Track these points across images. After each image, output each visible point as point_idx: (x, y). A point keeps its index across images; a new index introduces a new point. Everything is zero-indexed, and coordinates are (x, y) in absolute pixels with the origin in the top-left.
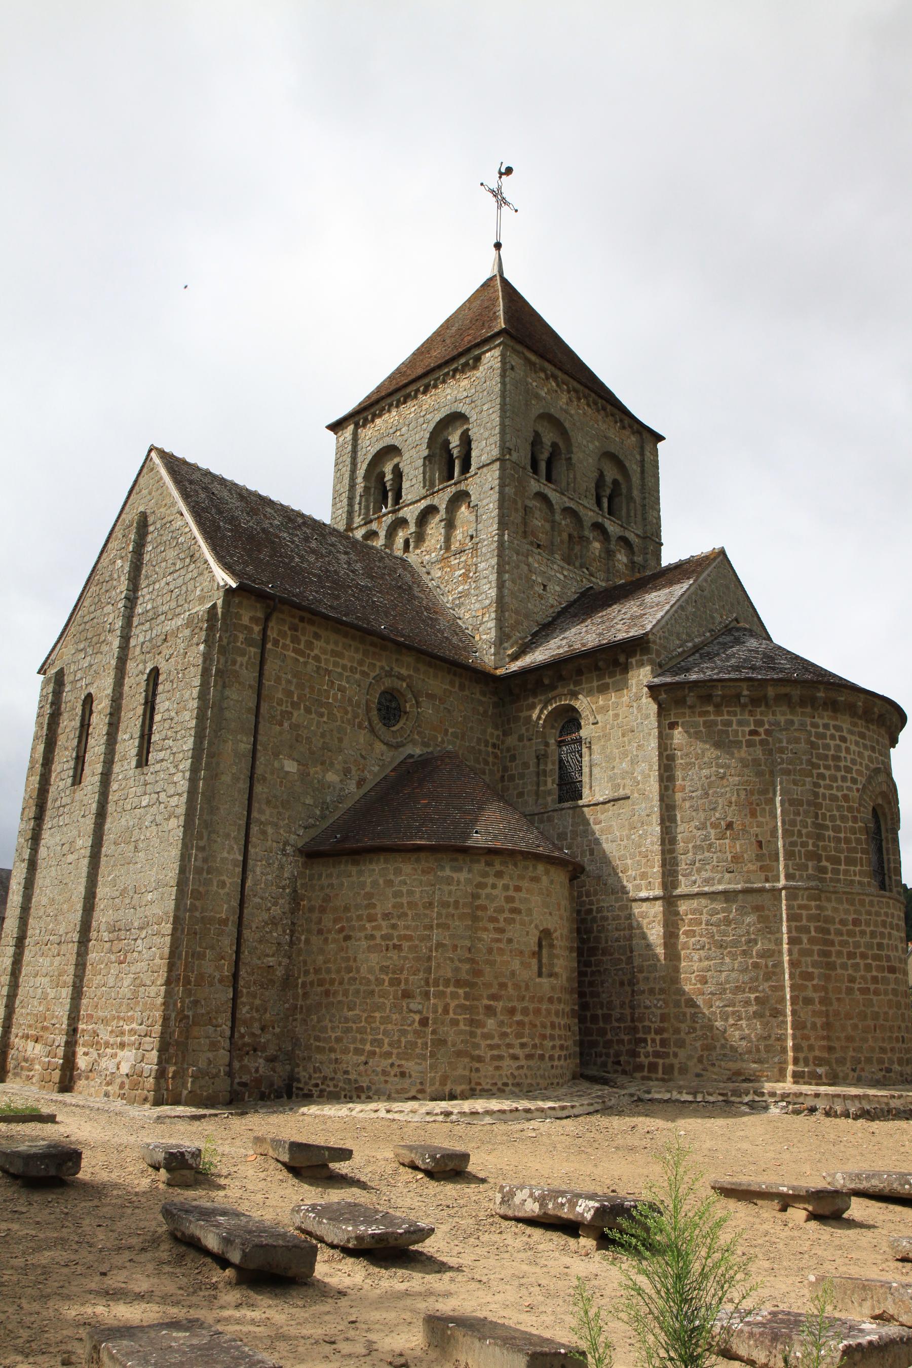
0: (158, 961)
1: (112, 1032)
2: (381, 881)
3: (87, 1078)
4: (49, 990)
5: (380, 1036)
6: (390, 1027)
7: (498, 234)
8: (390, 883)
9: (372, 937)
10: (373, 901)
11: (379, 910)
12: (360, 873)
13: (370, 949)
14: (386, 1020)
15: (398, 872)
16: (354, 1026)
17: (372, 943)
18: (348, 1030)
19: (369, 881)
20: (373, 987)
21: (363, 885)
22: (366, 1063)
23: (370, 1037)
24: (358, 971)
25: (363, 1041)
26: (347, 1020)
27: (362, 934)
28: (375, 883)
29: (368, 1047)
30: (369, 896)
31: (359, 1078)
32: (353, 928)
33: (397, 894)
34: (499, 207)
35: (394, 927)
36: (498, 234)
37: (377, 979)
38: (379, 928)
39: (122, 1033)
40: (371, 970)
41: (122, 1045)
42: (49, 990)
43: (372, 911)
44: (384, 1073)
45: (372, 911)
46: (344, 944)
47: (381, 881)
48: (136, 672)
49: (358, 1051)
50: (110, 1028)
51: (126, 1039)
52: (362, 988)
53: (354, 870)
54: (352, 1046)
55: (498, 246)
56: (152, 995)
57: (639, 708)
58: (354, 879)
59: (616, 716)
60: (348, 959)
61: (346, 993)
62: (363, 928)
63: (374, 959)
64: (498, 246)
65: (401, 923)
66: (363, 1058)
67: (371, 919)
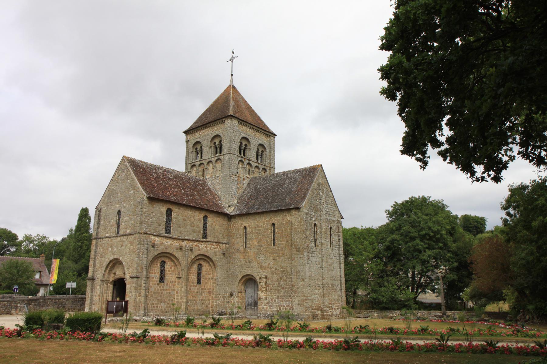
7: (232, 71)
34: (230, 60)
36: (232, 71)
55: (232, 75)
64: (232, 75)
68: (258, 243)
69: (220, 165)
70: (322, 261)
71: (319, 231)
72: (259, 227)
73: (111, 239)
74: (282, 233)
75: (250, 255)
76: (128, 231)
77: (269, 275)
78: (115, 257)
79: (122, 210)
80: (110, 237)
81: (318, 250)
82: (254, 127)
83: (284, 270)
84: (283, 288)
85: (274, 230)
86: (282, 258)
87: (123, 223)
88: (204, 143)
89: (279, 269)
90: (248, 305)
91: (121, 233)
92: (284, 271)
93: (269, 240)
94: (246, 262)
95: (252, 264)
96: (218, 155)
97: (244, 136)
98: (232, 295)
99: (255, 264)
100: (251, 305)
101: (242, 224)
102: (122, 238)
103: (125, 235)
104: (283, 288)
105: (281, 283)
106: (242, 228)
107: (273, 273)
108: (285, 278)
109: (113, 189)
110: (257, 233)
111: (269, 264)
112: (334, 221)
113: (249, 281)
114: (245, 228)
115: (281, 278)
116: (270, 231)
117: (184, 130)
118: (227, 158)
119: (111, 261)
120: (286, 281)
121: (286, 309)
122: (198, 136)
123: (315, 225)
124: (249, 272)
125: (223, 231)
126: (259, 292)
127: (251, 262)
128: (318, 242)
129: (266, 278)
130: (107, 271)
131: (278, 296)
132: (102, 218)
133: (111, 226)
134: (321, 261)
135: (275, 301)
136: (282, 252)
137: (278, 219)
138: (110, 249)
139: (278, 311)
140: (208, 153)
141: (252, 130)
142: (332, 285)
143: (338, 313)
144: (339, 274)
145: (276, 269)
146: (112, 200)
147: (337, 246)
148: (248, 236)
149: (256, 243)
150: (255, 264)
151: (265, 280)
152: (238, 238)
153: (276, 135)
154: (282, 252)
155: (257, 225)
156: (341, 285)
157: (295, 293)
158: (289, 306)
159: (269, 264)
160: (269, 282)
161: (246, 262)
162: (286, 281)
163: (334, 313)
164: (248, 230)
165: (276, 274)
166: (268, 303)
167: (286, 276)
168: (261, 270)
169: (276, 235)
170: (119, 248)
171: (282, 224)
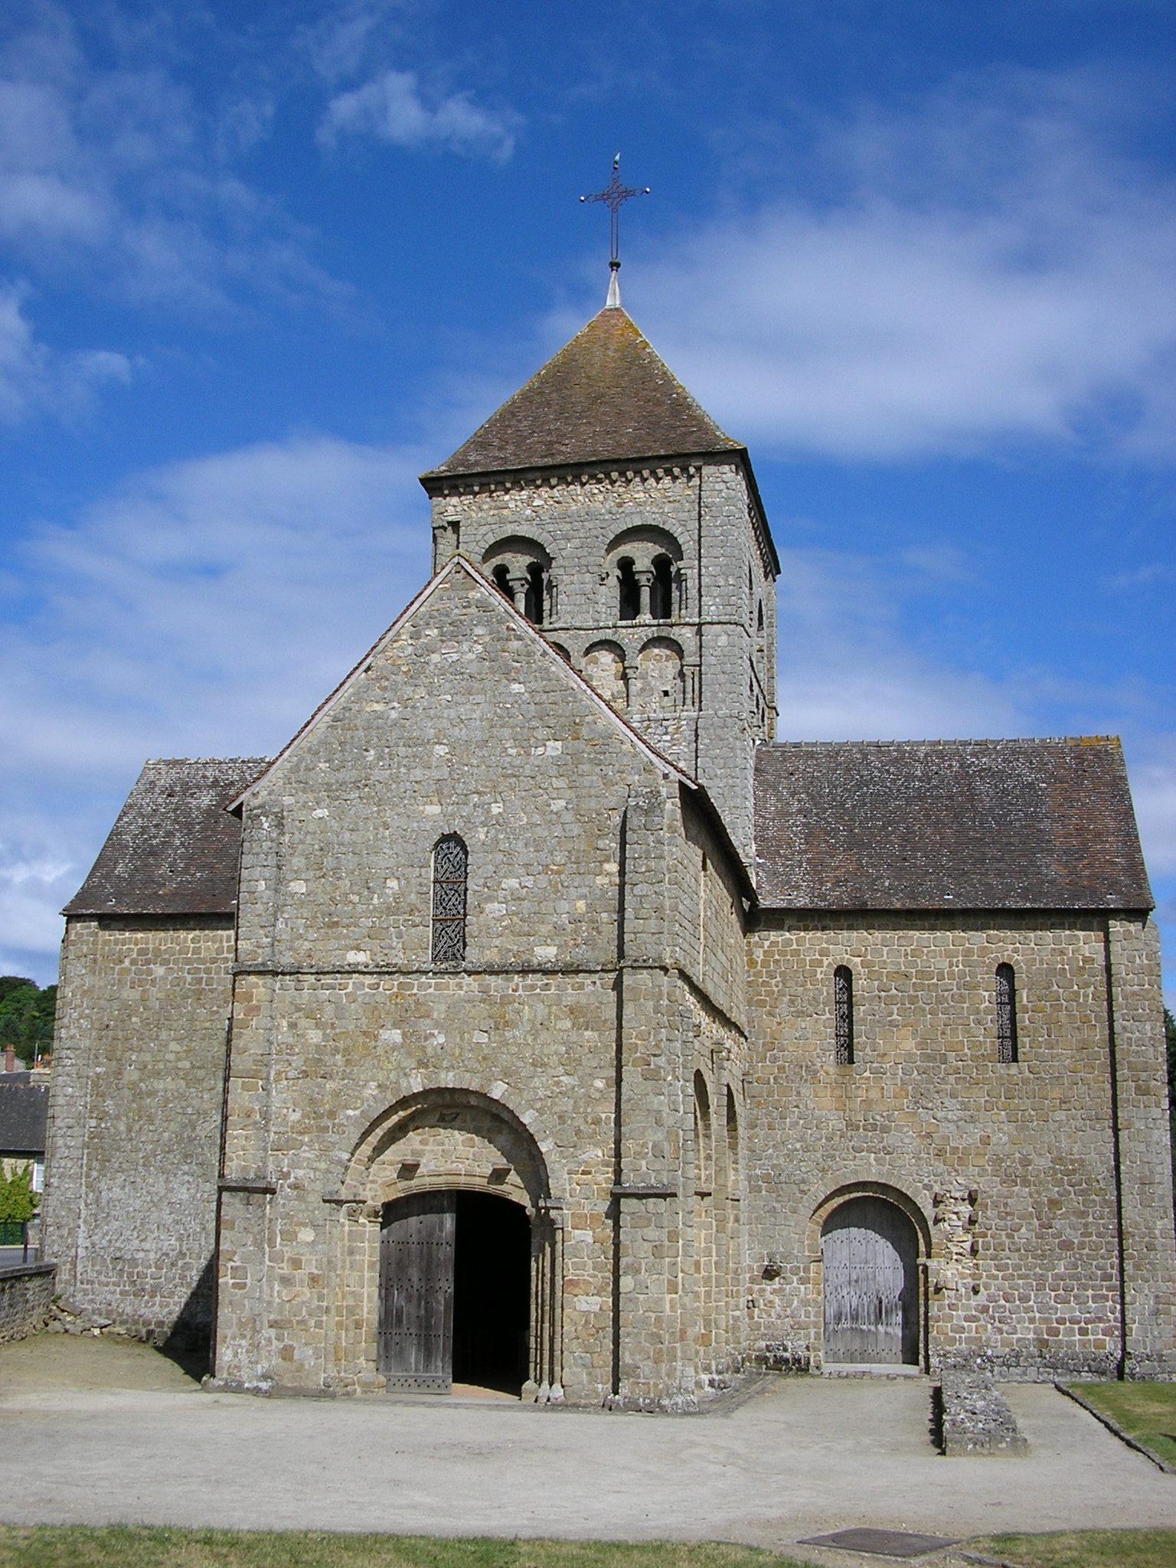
68: (921, 1045)
69: (671, 667)
72: (922, 974)
73: (393, 983)
74: (1057, 1008)
75: (874, 1094)
76: (547, 953)
77: (989, 1186)
78: (448, 1079)
79: (477, 837)
80: (385, 971)
83: (1067, 1169)
84: (1067, 1245)
85: (1012, 993)
86: (1061, 1115)
87: (494, 908)
88: (562, 550)
89: (1043, 1162)
90: (838, 1318)
91: (473, 955)
92: (1068, 1173)
93: (986, 1035)
94: (851, 1125)
95: (890, 1139)
96: (646, 617)
98: (769, 1274)
99: (906, 1138)
100: (855, 1318)
101: (824, 953)
102: (492, 981)
103: (524, 972)
104: (1067, 1245)
105: (1057, 1224)
106: (824, 972)
107: (1009, 1180)
108: (1075, 1201)
109: (380, 716)
110: (913, 1000)
111: (986, 1141)
113: (882, 1210)
114: (843, 973)
115: (1054, 1204)
116: (987, 997)
117: (422, 475)
118: (723, 640)
119: (403, 1103)
120: (1083, 1214)
121: (1083, 1332)
122: (521, 510)
124: (873, 1173)
126: (932, 1264)
127: (885, 1130)
129: (972, 1199)
130: (366, 1149)
131: (1041, 1277)
132: (298, 862)
133: (390, 911)
135: (1024, 1299)
136: (1057, 1093)
137: (1027, 948)
138: (395, 1035)
139: (1042, 1343)
140: (585, 598)
145: (1026, 1162)
146: (377, 775)
148: (859, 1012)
149: (910, 1045)
150: (906, 1138)
151: (965, 1209)
152: (800, 1014)
154: (1057, 1093)
155: (908, 964)
157: (1137, 1267)
158: (1100, 1320)
159: (986, 1141)
160: (989, 1217)
161: (851, 1125)
162: (1083, 1214)
164: (859, 984)
165: (1025, 1183)
166: (985, 1309)
167: (1083, 1192)
168: (941, 1168)
169: (1023, 1019)
170: (484, 1038)
171: (1052, 971)
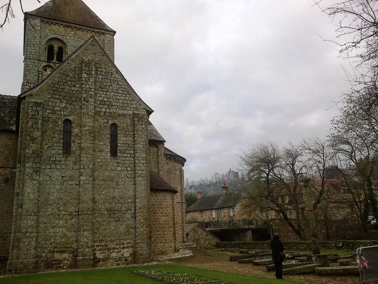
0: (142, 220)
1: (117, 244)
2: (163, 198)
3: (104, 261)
4: (67, 233)
5: (167, 238)
6: (168, 235)
8: (165, 199)
9: (162, 213)
10: (162, 203)
11: (163, 206)
12: (157, 196)
13: (162, 216)
14: (167, 234)
15: (166, 196)
16: (160, 236)
17: (162, 214)
18: (158, 237)
19: (160, 198)
20: (164, 225)
21: (158, 199)
22: (164, 245)
23: (164, 239)
24: (159, 221)
25: (162, 240)
26: (157, 235)
27: (160, 212)
28: (161, 199)
29: (164, 241)
30: (160, 202)
31: (162, 250)
32: (156, 210)
33: (167, 202)
35: (167, 210)
37: (164, 224)
38: (164, 210)
39: (124, 244)
40: (163, 221)
41: (124, 248)
42: (67, 233)
43: (162, 206)
44: (168, 247)
45: (162, 206)
46: (154, 215)
47: (163, 198)
48: (102, 121)
49: (161, 243)
50: (116, 243)
51: (126, 246)
52: (161, 226)
53: (154, 195)
54: (159, 241)
56: (142, 231)
57: (161, 158)
58: (155, 197)
59: (153, 158)
60: (156, 218)
61: (156, 228)
62: (159, 210)
63: (163, 218)
65: (168, 209)
66: (163, 244)
67: (162, 208)
70: (81, 175)
71: (76, 131)
81: (71, 159)
82: (72, 25)
97: (55, 36)
112: (124, 116)
123: (67, 122)
125: (7, 152)
128: (74, 147)
134: (78, 174)
141: (70, 29)
142: (107, 210)
143: (127, 255)
144: (131, 193)
147: (132, 152)
153: (115, 32)
156: (135, 210)
163: (114, 255)
